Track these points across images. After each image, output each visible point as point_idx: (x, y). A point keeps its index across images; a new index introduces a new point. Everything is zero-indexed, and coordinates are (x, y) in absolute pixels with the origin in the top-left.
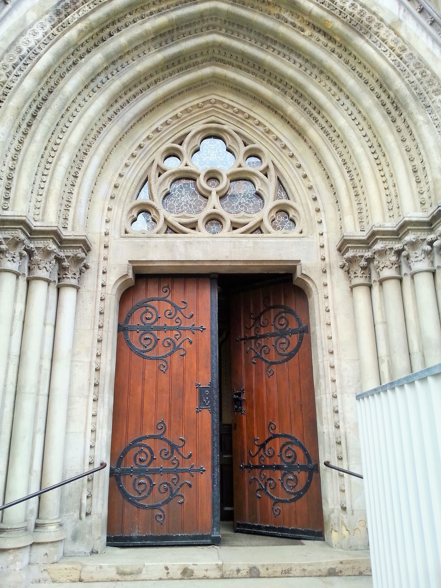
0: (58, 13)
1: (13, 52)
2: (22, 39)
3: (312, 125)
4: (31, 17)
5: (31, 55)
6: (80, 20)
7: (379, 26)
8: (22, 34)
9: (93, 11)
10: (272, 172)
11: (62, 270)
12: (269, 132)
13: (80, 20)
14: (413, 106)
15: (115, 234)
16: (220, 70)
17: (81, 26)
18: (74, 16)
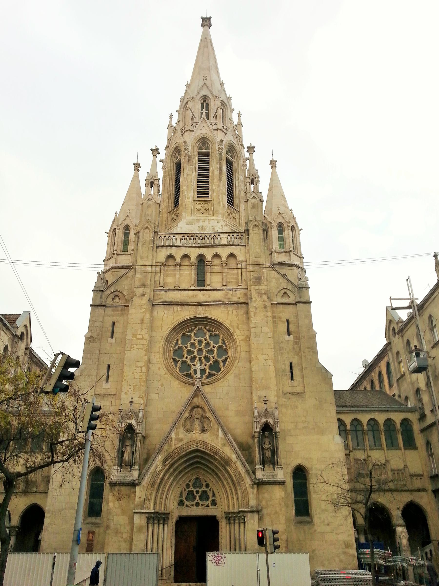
0: (164, 462)
1: (155, 473)
2: (157, 469)
3: (220, 481)
4: (158, 463)
5: (159, 473)
6: (168, 464)
7: (232, 463)
8: (157, 468)
9: (171, 461)
10: (211, 490)
11: (164, 520)
12: (211, 480)
13: (168, 464)
14: (237, 485)
15: (175, 508)
16: (199, 465)
17: (168, 465)
18: (167, 463)
